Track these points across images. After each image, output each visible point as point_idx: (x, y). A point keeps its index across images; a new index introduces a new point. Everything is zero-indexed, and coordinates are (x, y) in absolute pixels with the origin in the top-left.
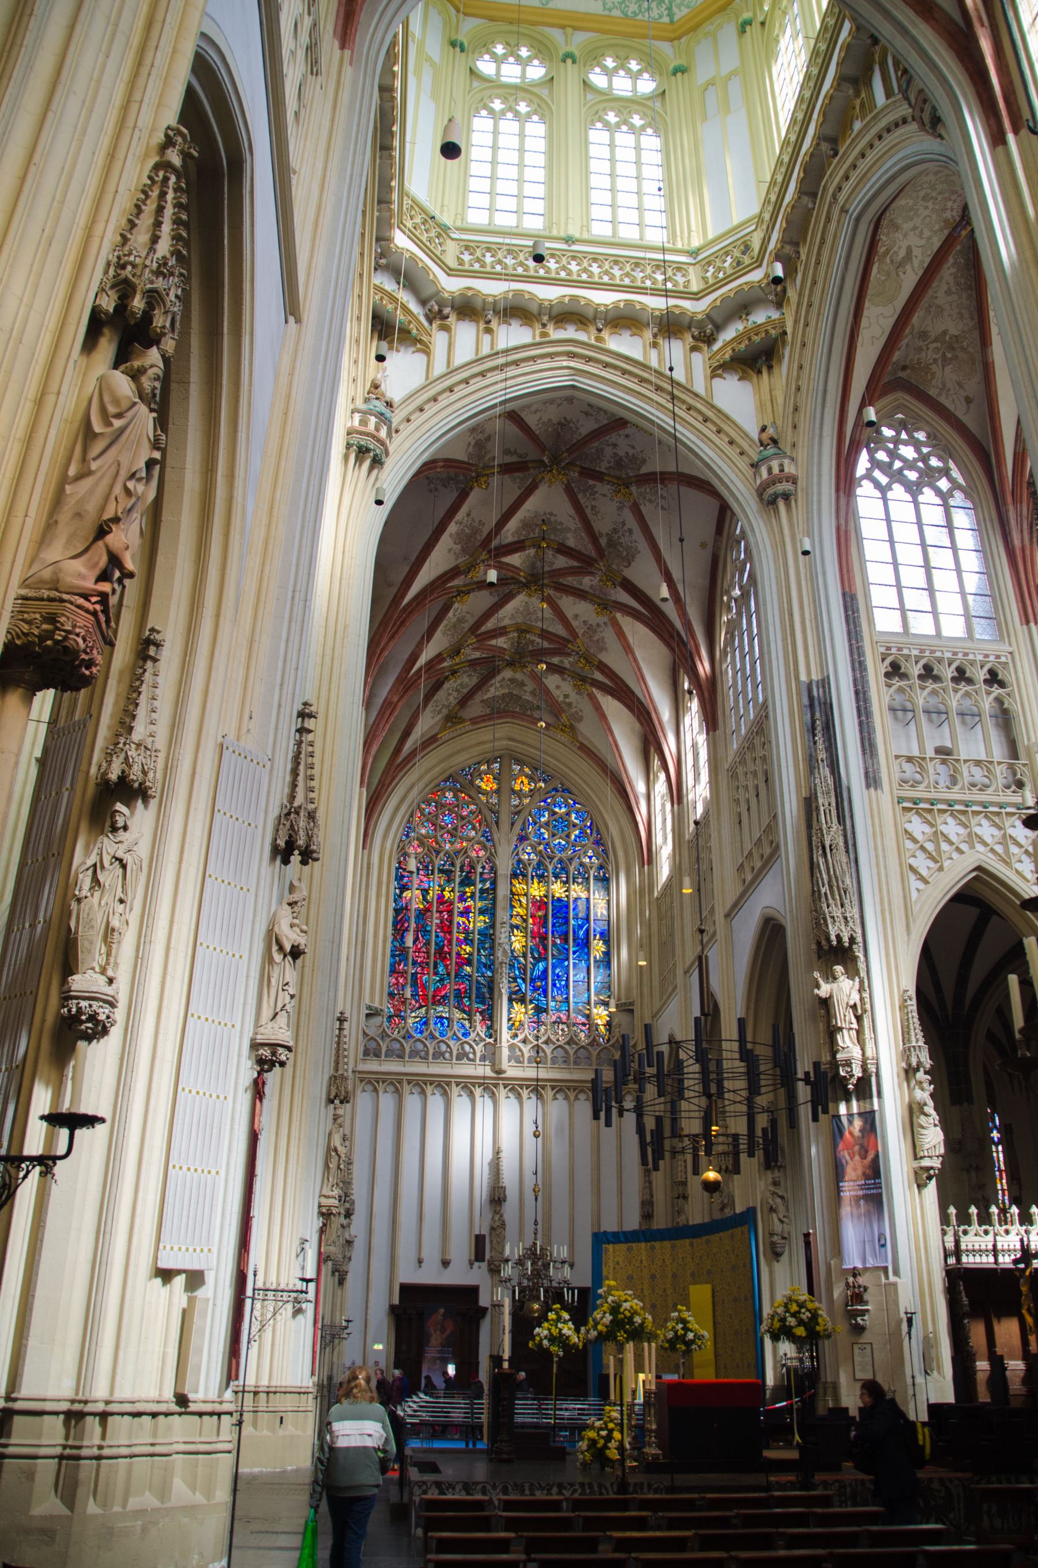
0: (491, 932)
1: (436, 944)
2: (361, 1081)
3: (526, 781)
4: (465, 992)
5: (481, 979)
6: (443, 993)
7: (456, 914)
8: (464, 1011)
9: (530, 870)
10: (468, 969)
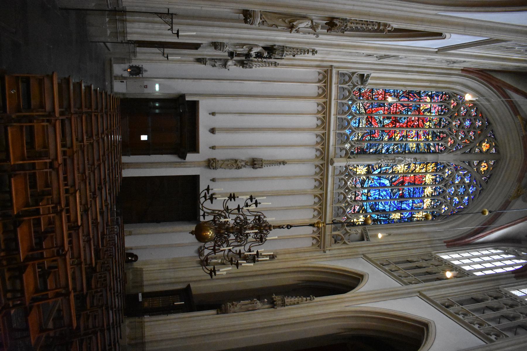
0: (407, 152)
1: (401, 118)
2: (325, 72)
3: (485, 169)
4: (374, 137)
5: (380, 147)
6: (373, 123)
7: (417, 130)
8: (362, 137)
9: (440, 174)
10: (386, 139)
